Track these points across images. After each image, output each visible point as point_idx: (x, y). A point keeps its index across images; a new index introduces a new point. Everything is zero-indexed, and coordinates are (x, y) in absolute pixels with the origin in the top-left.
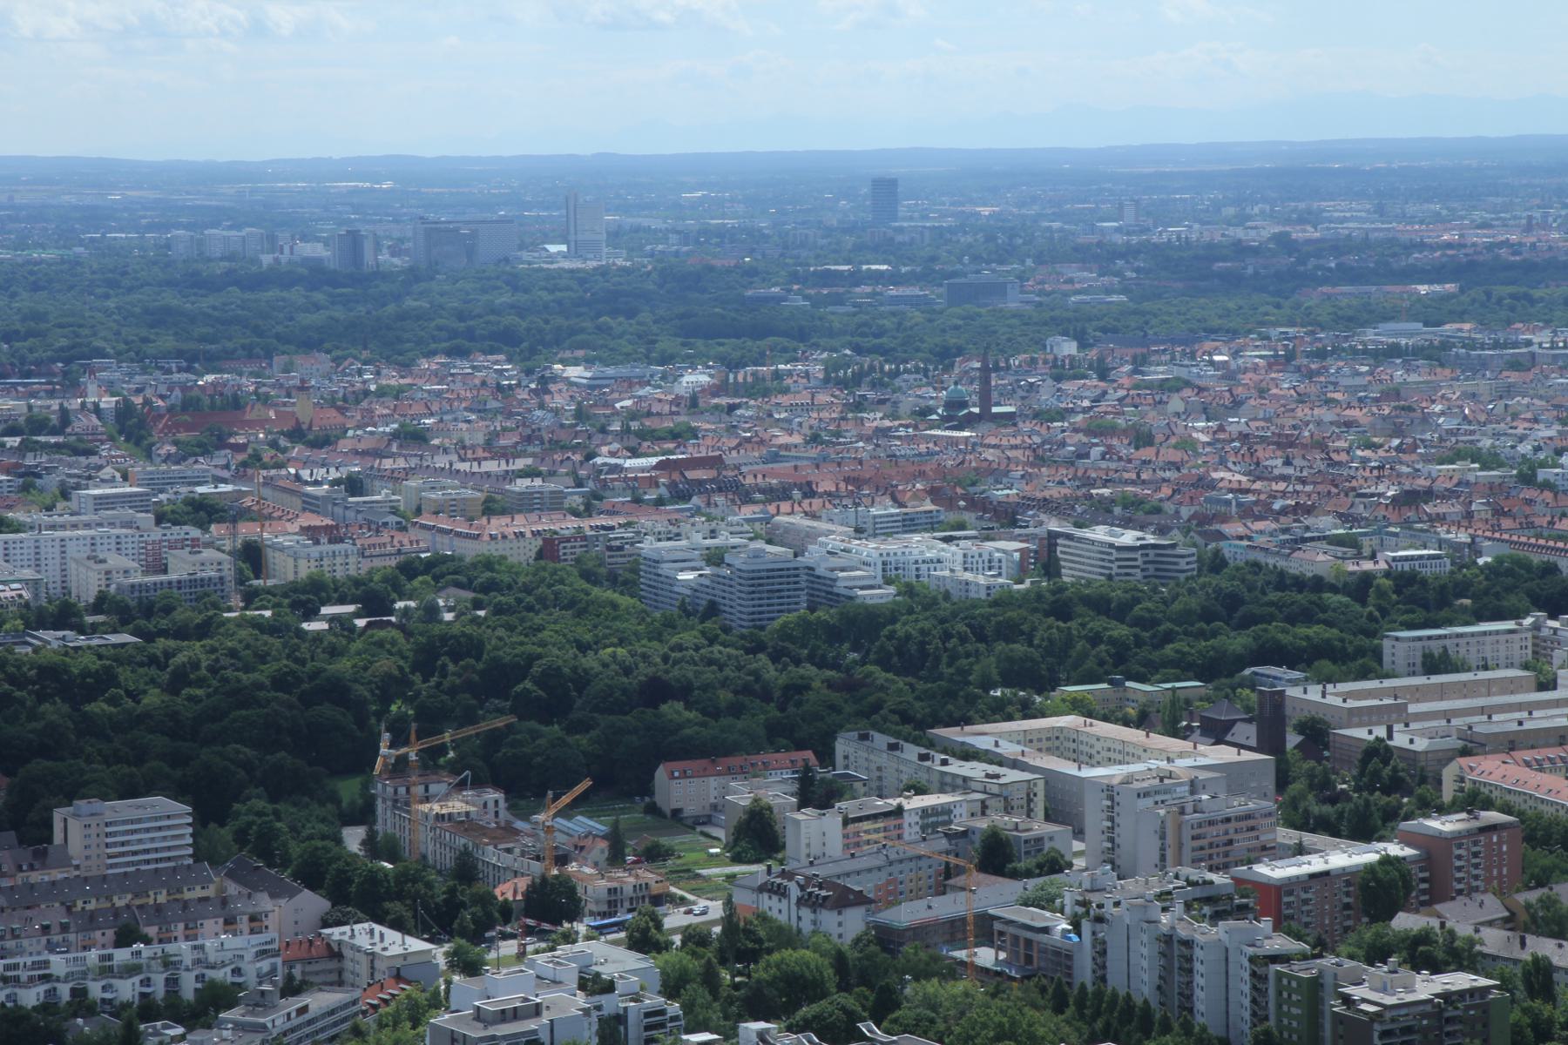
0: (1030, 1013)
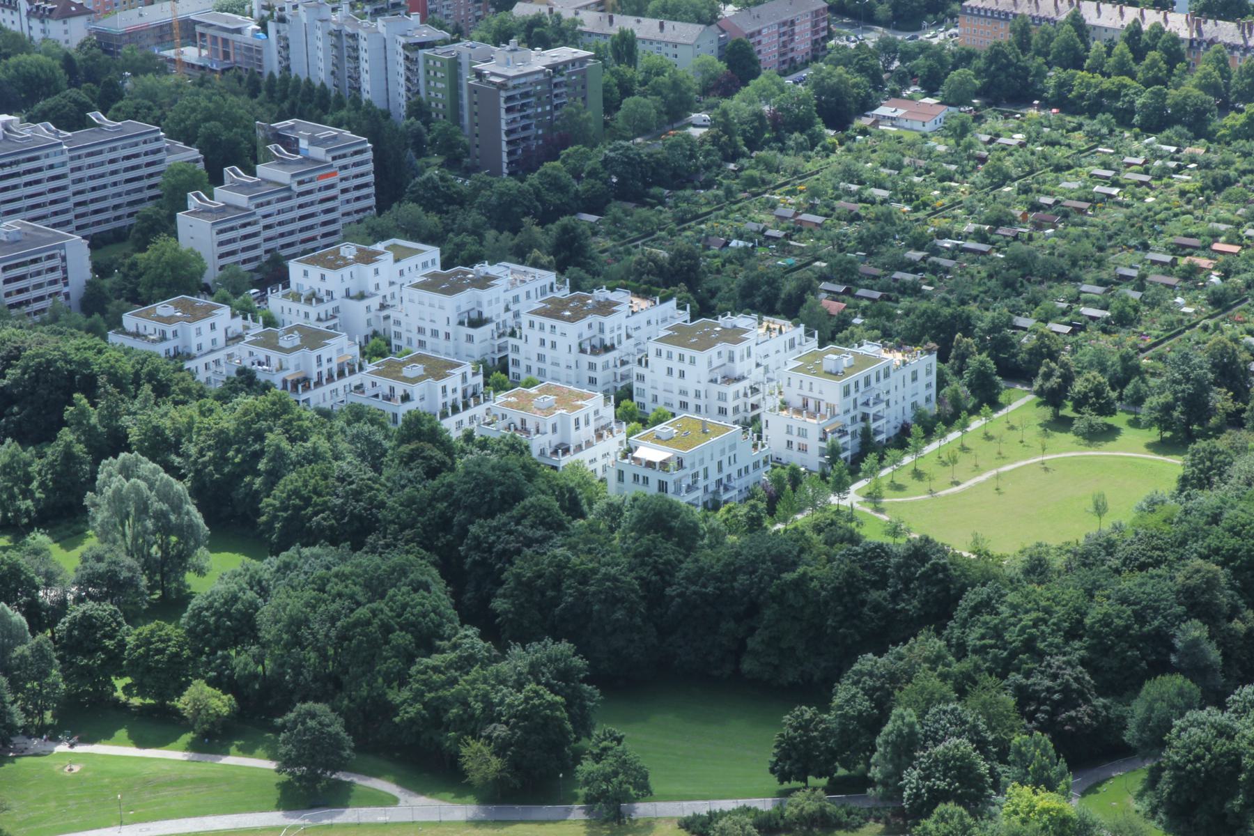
0: (231, 98)
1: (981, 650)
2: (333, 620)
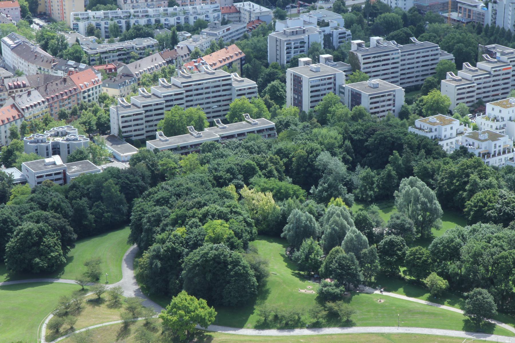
0: (469, 34)
2: (492, 255)
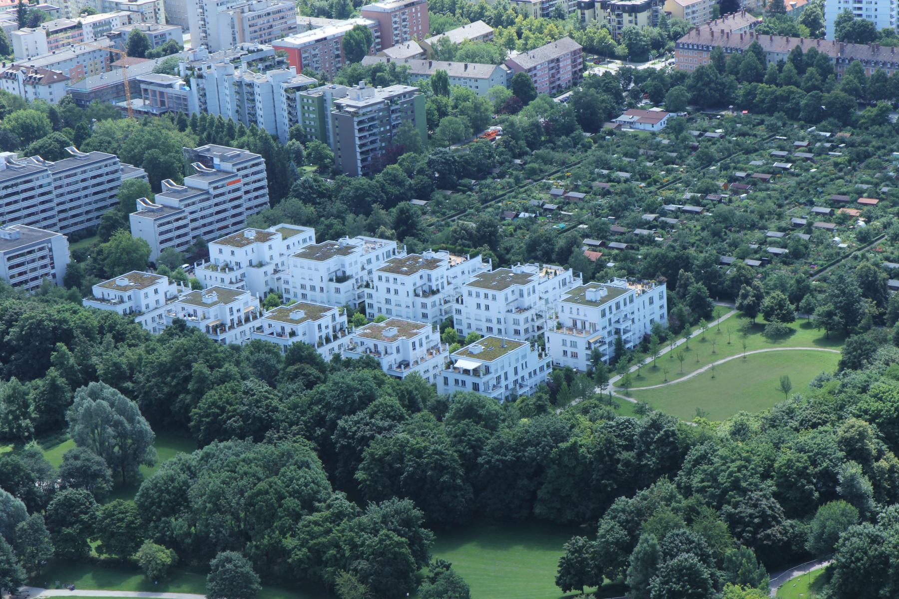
1: (702, 490)
